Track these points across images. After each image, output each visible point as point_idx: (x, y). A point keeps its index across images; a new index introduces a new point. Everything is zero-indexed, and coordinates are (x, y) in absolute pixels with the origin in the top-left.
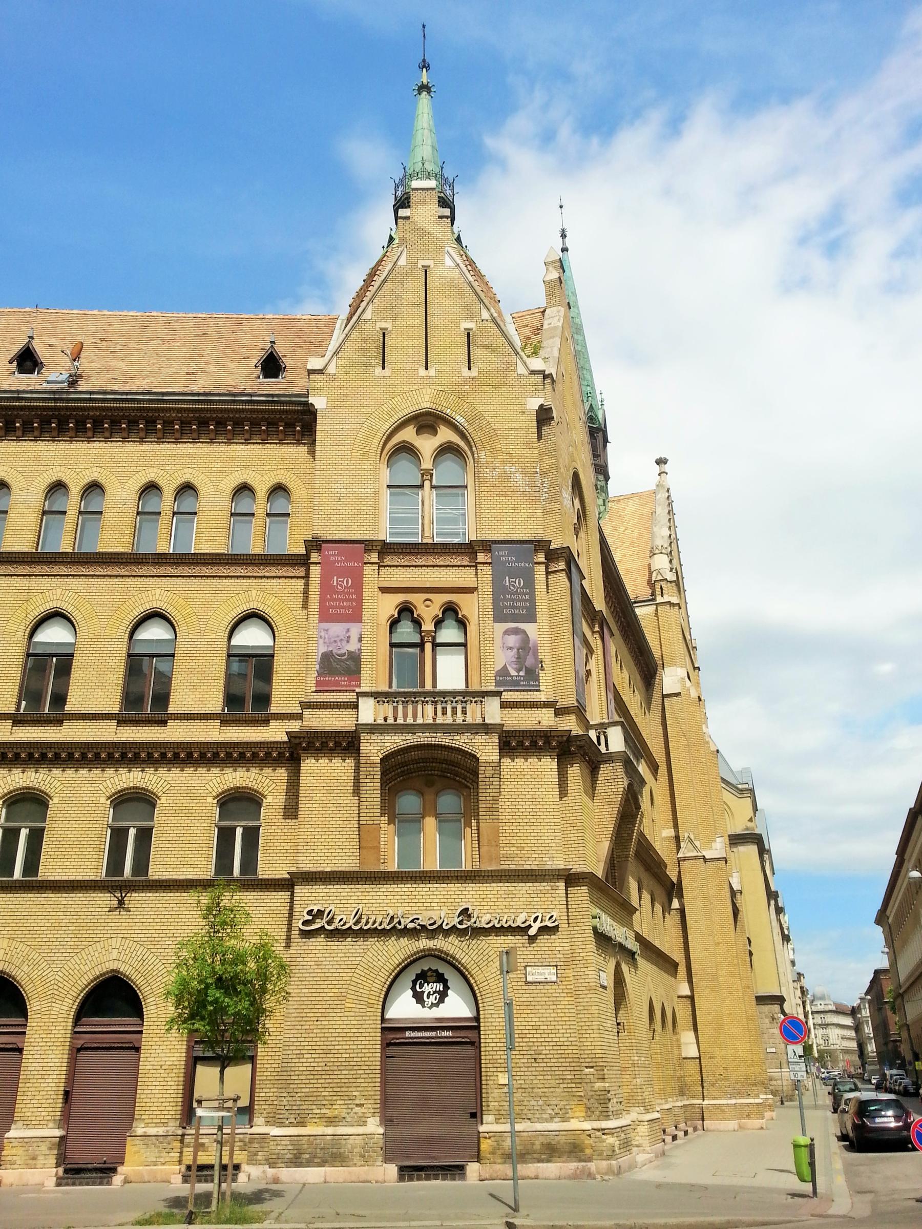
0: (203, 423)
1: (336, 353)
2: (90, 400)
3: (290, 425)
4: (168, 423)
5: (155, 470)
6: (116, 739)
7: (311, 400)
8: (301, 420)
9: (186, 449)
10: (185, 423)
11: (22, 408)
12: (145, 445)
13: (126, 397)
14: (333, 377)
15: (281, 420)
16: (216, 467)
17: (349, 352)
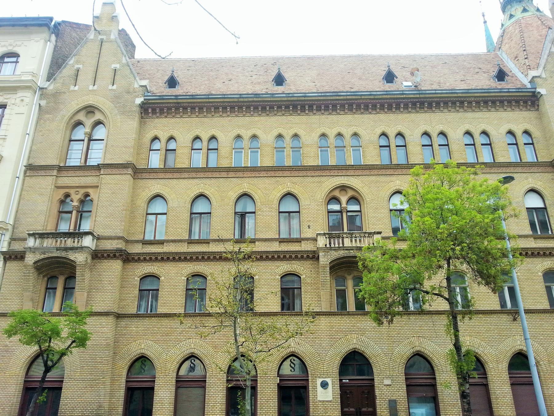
0: (438, 104)
1: (544, 68)
2: (435, 93)
3: (525, 102)
4: (470, 103)
5: (468, 125)
6: (280, 249)
7: (538, 90)
8: (530, 100)
9: (479, 115)
10: (478, 103)
11: (404, 98)
12: (460, 114)
13: (453, 91)
14: (545, 79)
15: (521, 100)
16: (499, 123)
17: (549, 67)
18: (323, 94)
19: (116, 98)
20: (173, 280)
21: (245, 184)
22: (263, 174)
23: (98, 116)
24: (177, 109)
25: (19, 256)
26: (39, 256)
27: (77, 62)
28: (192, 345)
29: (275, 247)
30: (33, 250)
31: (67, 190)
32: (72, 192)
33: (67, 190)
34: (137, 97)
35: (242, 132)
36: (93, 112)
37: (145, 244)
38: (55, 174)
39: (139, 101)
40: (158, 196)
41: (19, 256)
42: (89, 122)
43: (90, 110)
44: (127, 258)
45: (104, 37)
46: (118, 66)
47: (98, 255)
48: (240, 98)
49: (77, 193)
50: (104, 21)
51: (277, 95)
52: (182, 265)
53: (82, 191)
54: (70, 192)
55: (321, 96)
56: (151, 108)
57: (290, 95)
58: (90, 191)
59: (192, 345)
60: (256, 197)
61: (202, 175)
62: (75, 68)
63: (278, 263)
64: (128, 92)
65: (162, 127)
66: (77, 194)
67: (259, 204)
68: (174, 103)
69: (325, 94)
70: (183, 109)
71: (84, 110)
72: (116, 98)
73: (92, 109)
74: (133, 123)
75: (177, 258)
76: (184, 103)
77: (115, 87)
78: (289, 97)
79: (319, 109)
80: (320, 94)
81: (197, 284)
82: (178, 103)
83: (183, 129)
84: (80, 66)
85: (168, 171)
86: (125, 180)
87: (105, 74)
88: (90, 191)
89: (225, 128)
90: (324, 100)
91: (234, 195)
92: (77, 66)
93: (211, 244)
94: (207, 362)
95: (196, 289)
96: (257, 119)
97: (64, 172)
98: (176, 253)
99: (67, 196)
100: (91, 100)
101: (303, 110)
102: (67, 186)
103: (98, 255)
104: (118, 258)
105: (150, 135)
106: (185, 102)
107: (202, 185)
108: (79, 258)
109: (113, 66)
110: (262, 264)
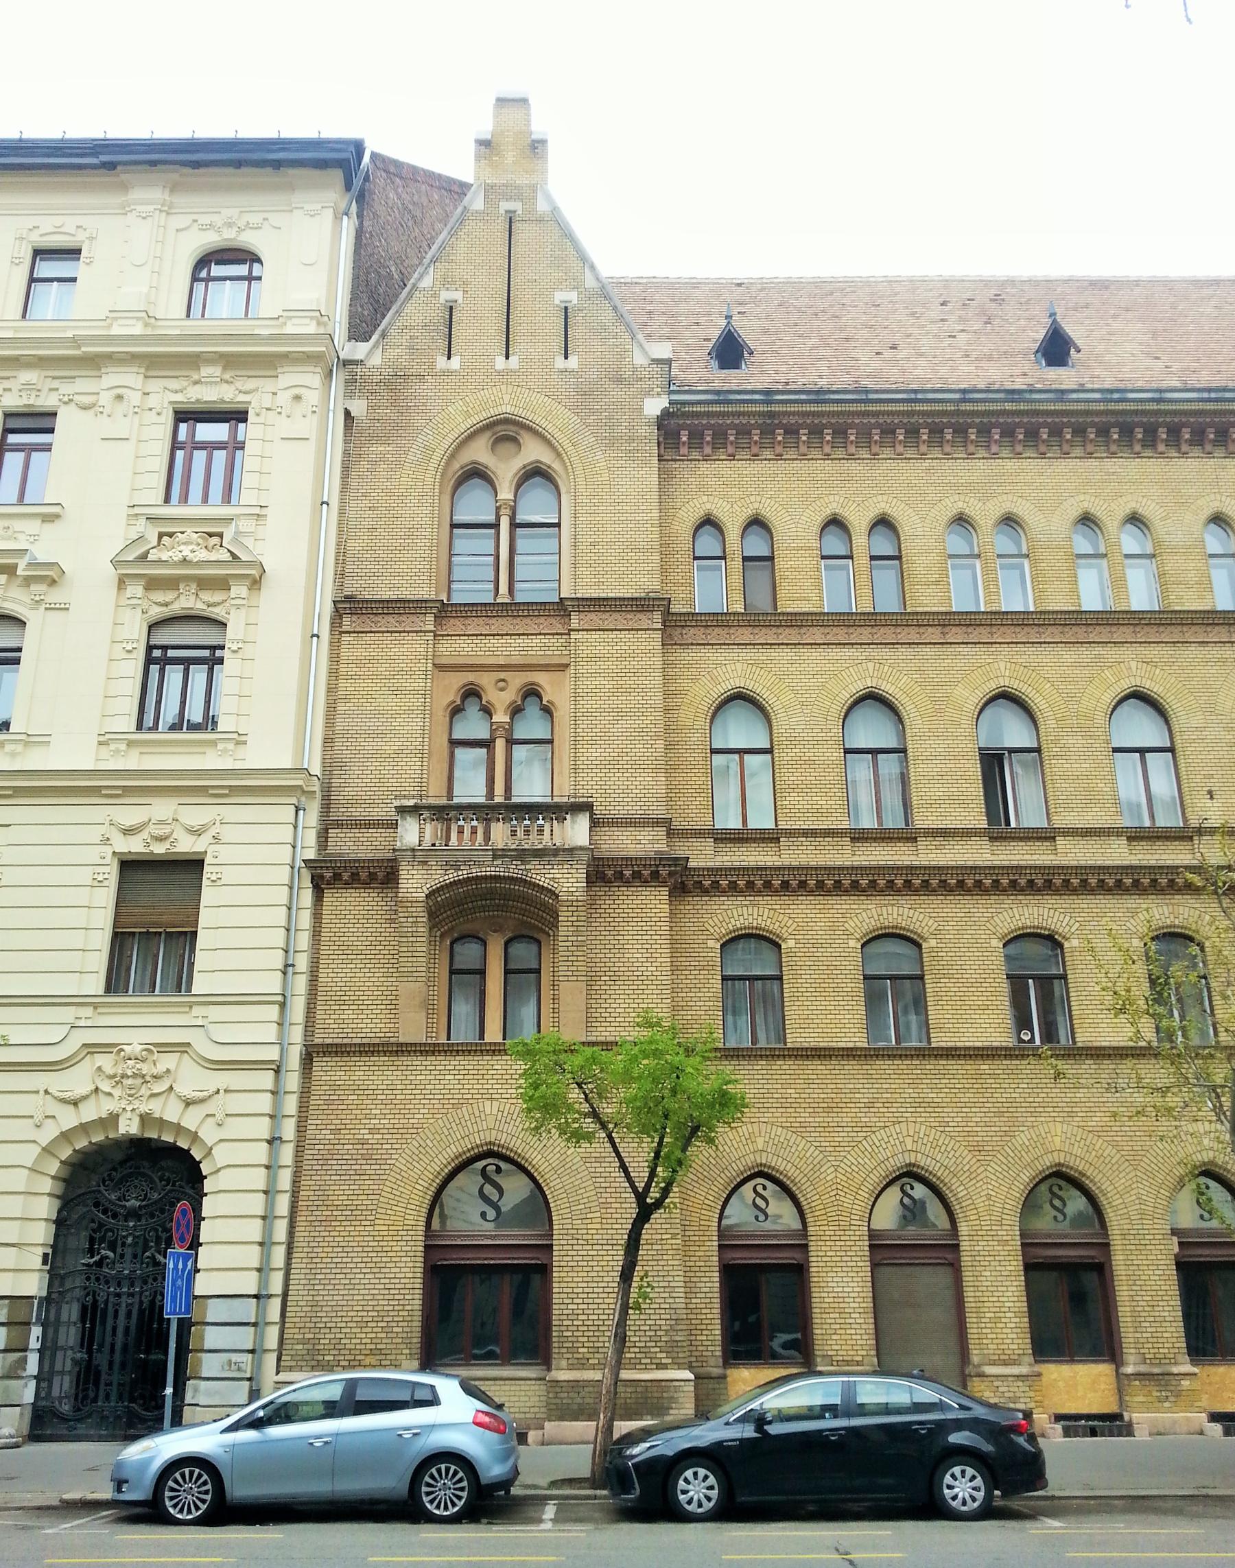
18: (1213, 395)
19: (584, 397)
20: (823, 947)
21: (1002, 665)
22: (1050, 634)
23: (532, 452)
24: (768, 431)
25: (364, 875)
26: (439, 876)
27: (446, 282)
28: (909, 1141)
29: (1119, 854)
30: (420, 855)
31: (471, 677)
32: (486, 681)
33: (471, 677)
34: (648, 393)
35: (973, 508)
36: (514, 440)
37: (722, 840)
38: (432, 628)
39: (655, 406)
40: (740, 697)
41: (382, 875)
42: (506, 470)
43: (505, 431)
44: (682, 882)
45: (517, 206)
46: (572, 297)
47: (605, 873)
48: (964, 400)
49: (502, 685)
50: (510, 157)
51: (1074, 396)
52: (841, 905)
53: (517, 681)
54: (479, 682)
55: (1209, 400)
56: (688, 432)
57: (1116, 396)
58: (541, 678)
59: (909, 1141)
60: (1038, 702)
61: (865, 634)
62: (442, 301)
63: (1131, 902)
64: (619, 380)
65: (728, 487)
66: (502, 690)
67: (1052, 723)
68: (760, 414)
69: (1220, 395)
70: (786, 433)
71: (488, 434)
72: (584, 397)
73: (510, 430)
74: (642, 476)
75: (830, 883)
76: (789, 414)
77: (573, 362)
78: (1111, 400)
79: (1198, 439)
80: (1205, 395)
81: (895, 960)
82: (771, 415)
83: (792, 494)
84: (458, 295)
85: (766, 621)
86: (640, 645)
87: (536, 320)
88: (541, 678)
89: (919, 492)
90: (1215, 413)
91: (972, 698)
92: (445, 296)
93: (922, 843)
94: (957, 1190)
95: (895, 977)
96: (1011, 465)
97: (455, 621)
98: (829, 870)
99: (471, 693)
100: (506, 403)
101: (1150, 441)
102: (472, 666)
103: (605, 873)
104: (664, 883)
105: (689, 514)
106: (794, 414)
107: (871, 665)
108: (568, 881)
109: (560, 297)
110: (1085, 904)
